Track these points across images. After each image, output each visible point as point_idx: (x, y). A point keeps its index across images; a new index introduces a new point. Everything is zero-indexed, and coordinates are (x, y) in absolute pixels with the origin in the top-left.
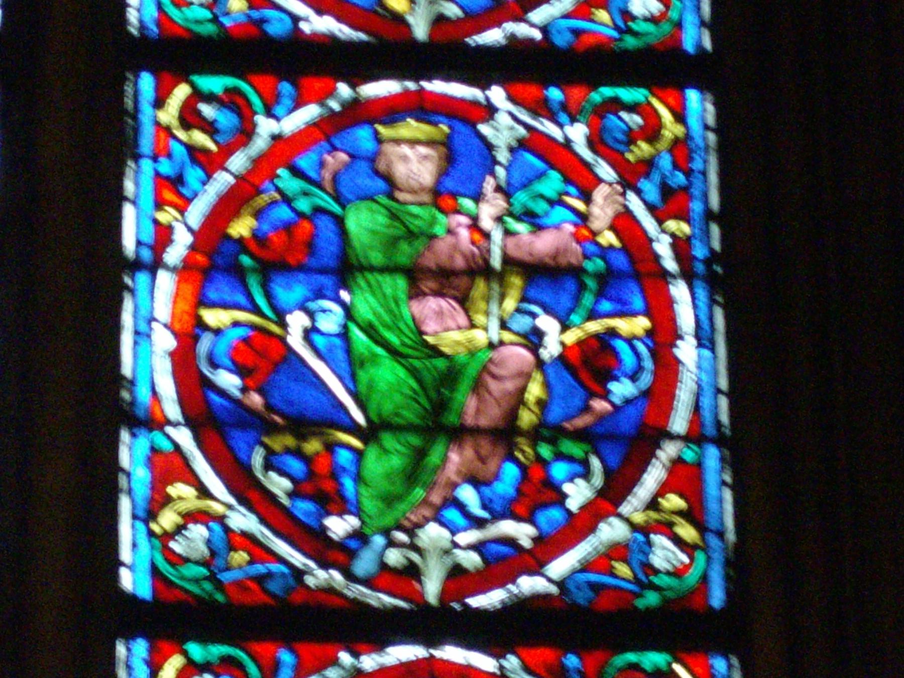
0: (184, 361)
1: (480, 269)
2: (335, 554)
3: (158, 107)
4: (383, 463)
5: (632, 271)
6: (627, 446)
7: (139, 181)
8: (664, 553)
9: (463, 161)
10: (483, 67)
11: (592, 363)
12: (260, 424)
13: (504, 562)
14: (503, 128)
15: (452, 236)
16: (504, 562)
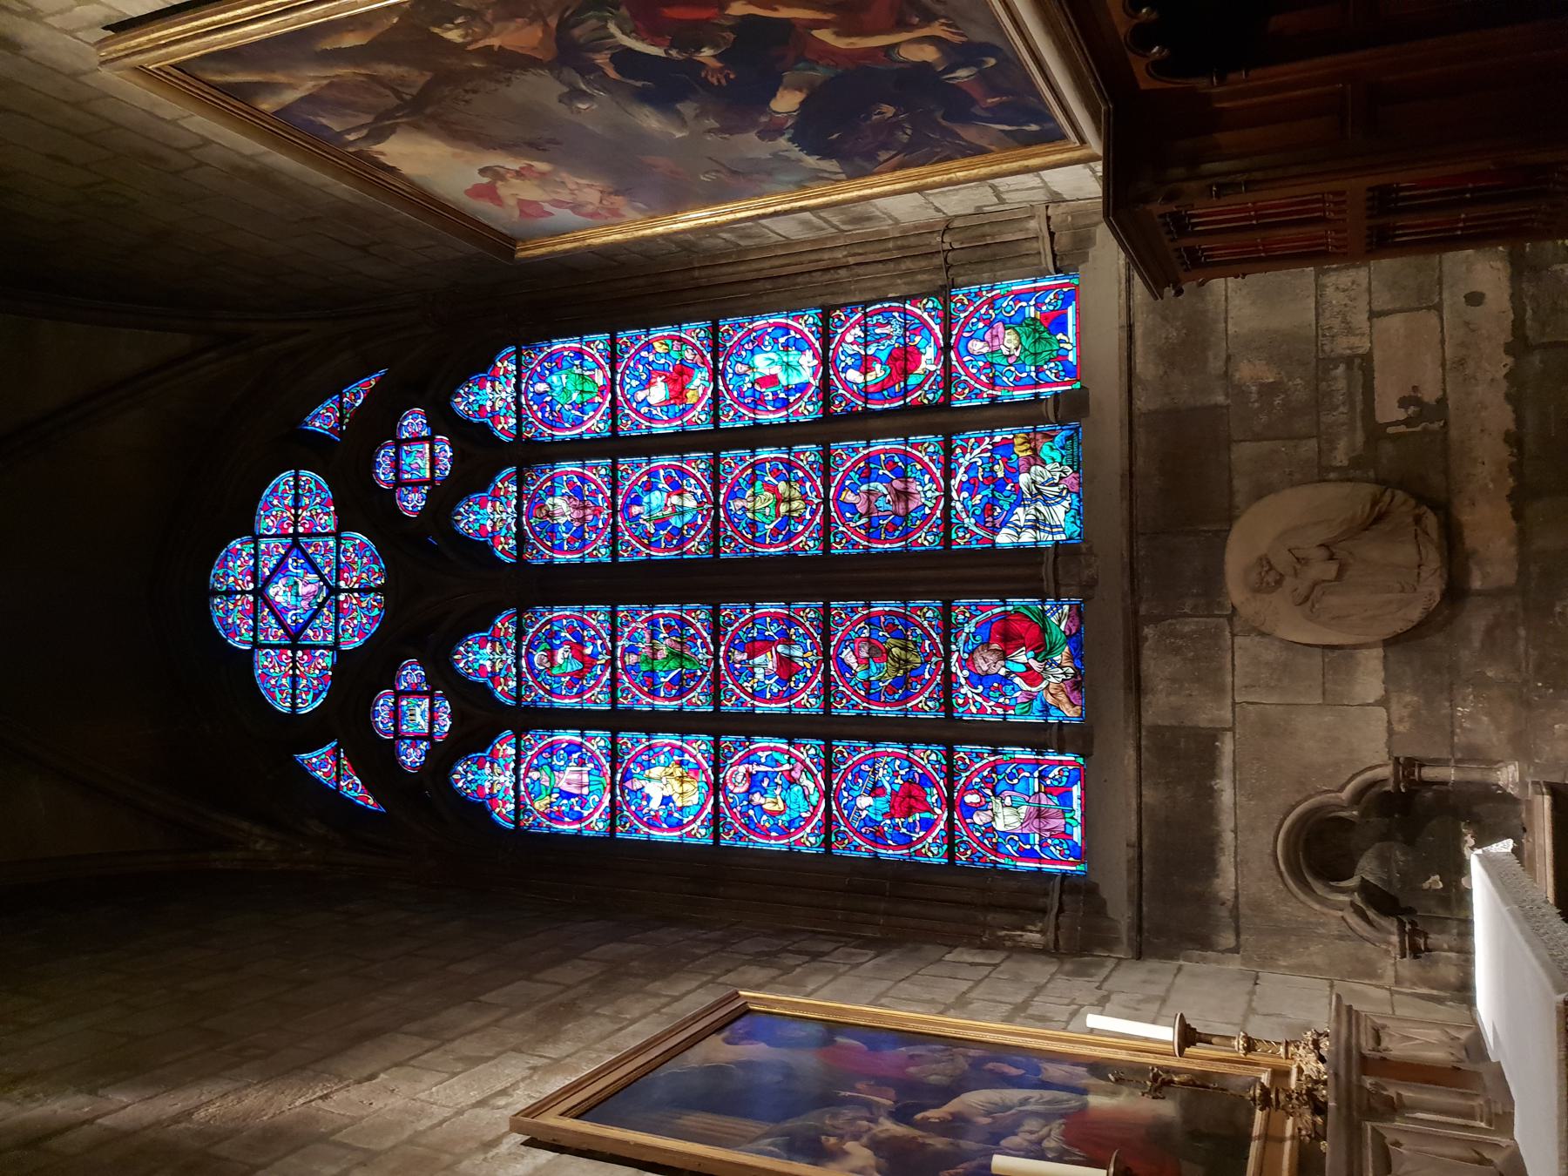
0: (670, 700)
1: (652, 647)
2: (704, 673)
3: (624, 703)
4: (688, 665)
5: (652, 621)
6: (683, 623)
7: (637, 707)
8: (702, 616)
9: (632, 650)
10: (615, 647)
11: (668, 627)
12: (681, 687)
13: (705, 645)
14: (627, 644)
15: (646, 652)
16: (705, 645)
